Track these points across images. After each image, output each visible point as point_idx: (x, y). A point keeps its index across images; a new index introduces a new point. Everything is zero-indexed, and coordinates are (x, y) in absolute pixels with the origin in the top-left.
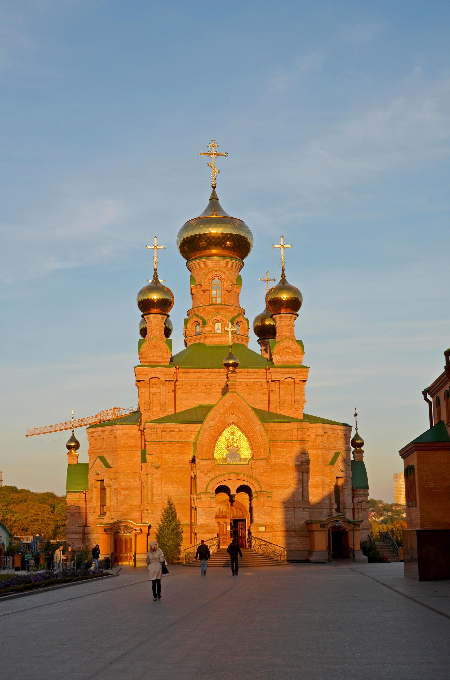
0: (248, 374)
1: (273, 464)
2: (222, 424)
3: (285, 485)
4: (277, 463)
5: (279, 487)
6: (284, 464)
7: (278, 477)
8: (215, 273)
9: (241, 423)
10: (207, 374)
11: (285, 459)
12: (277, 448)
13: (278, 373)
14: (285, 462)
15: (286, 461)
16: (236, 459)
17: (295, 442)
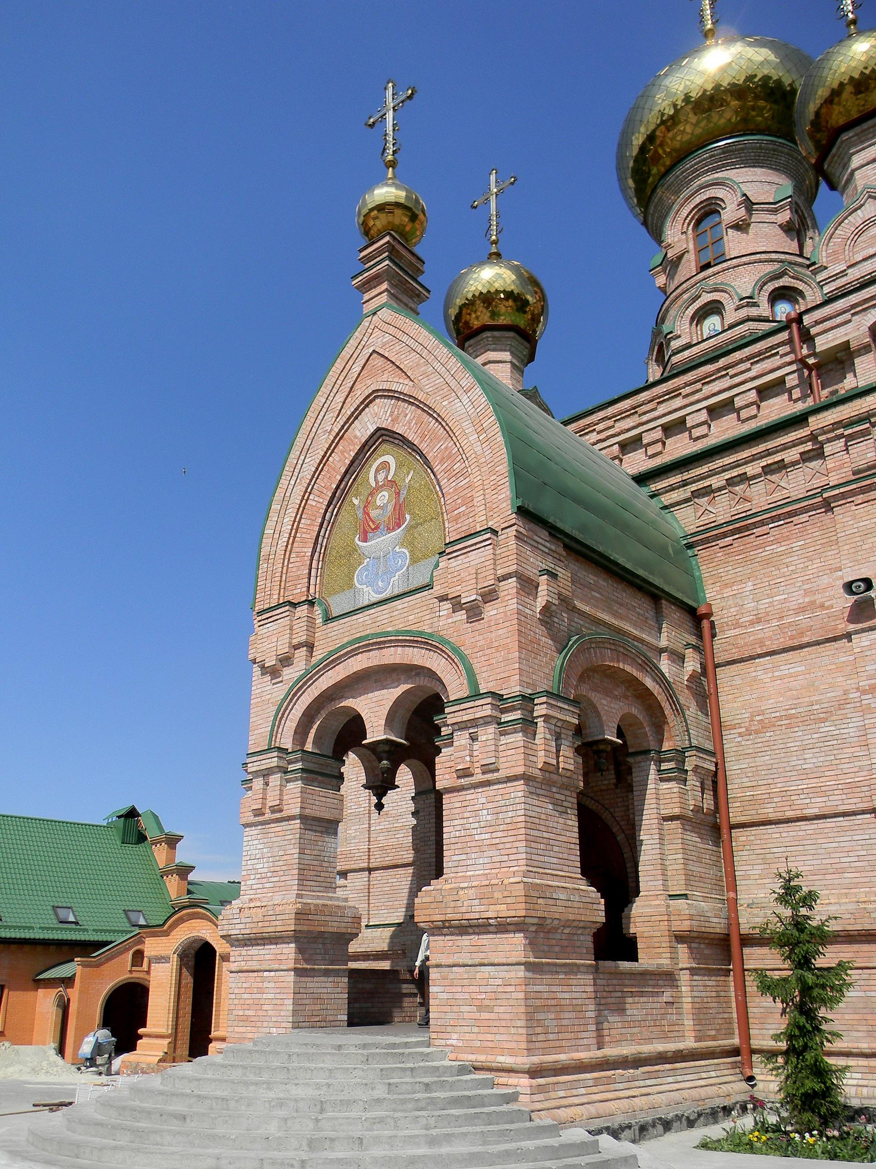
0: (731, 372)
1: (752, 623)
2: (342, 452)
3: (817, 702)
4: (767, 614)
5: (789, 717)
6: (802, 609)
7: (776, 674)
8: (697, 200)
9: (407, 415)
10: (601, 427)
11: (805, 587)
12: (763, 546)
13: (839, 320)
14: (807, 600)
15: (807, 592)
16: (392, 580)
17: (843, 496)
